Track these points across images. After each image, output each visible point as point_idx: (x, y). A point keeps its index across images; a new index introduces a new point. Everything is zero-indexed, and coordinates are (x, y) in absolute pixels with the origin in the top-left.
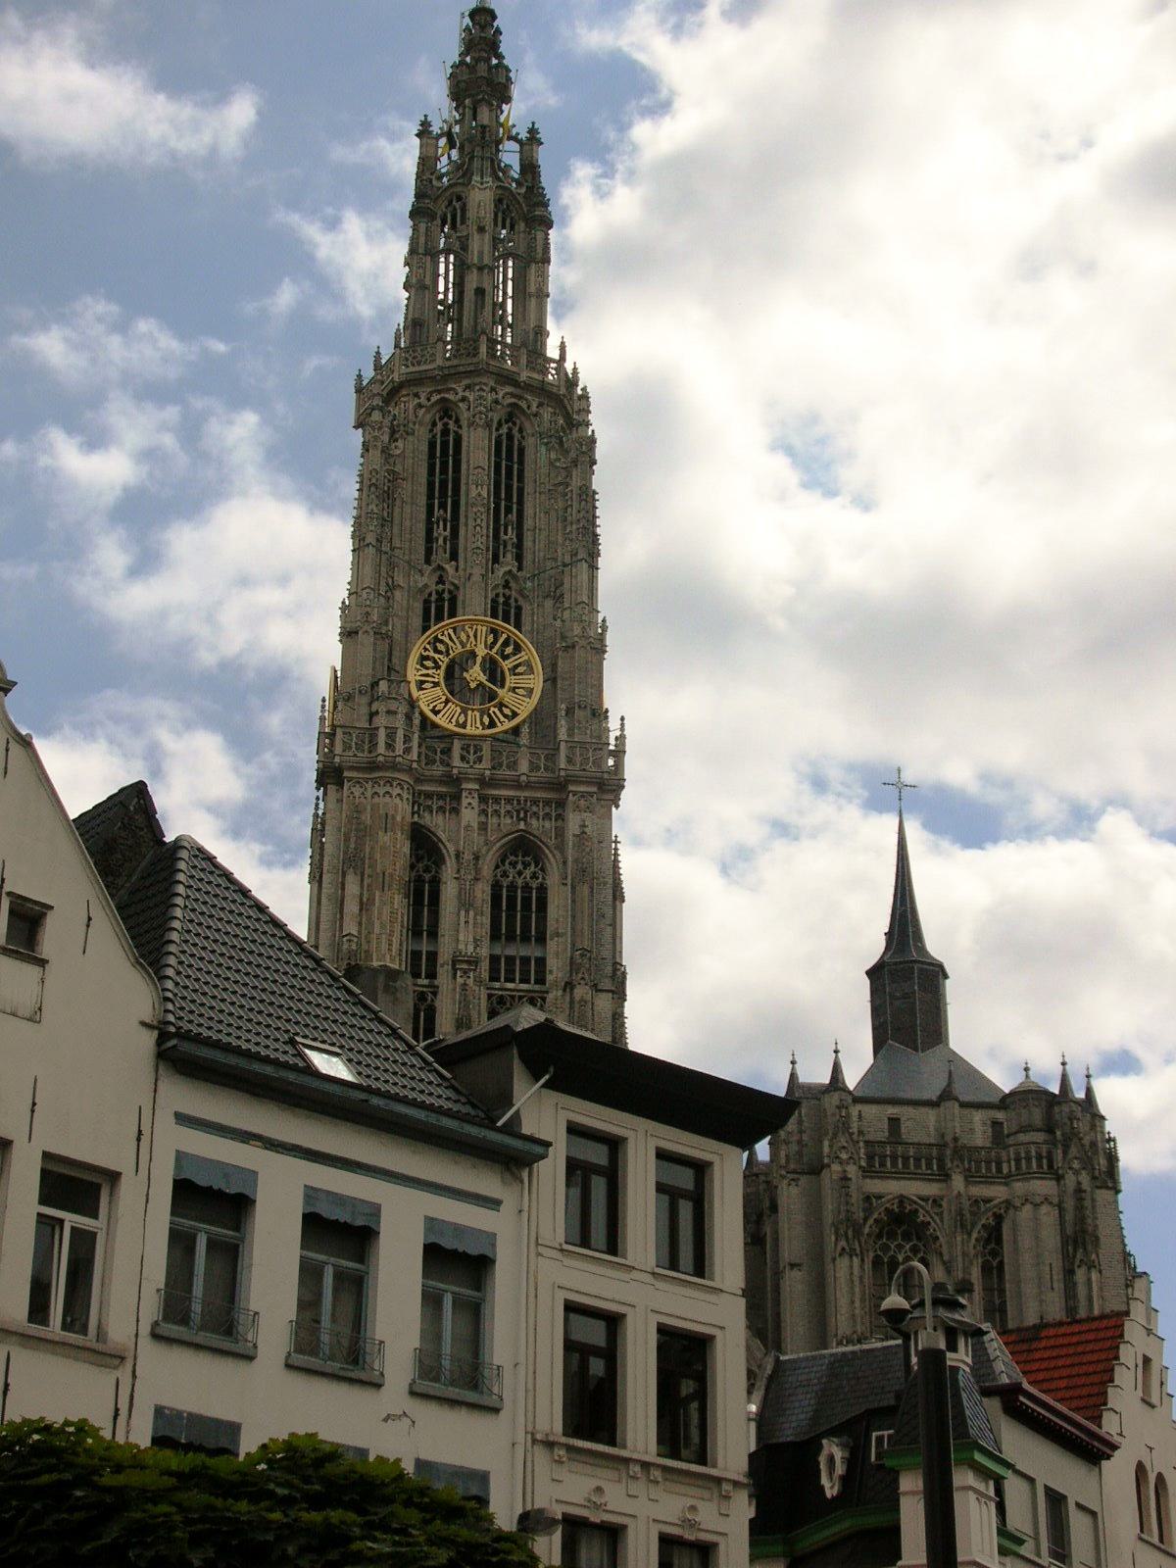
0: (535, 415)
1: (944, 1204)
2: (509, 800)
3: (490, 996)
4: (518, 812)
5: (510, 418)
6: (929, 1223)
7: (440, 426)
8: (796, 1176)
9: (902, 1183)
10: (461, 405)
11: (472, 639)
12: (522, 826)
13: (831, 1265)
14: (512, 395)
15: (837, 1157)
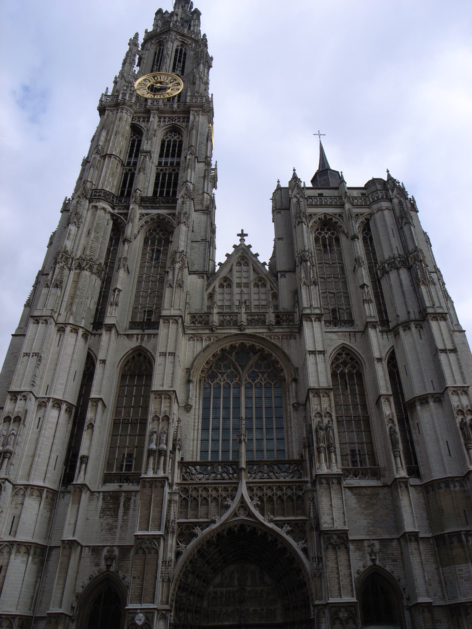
0: (190, 45)
1: (344, 215)
2: (169, 118)
3: (157, 169)
4: (172, 120)
5: (182, 46)
6: (337, 222)
7: (158, 48)
8: (279, 211)
9: (325, 209)
10: (164, 40)
11: (159, 79)
12: (173, 122)
13: (294, 230)
14: (182, 39)
15: (295, 196)
